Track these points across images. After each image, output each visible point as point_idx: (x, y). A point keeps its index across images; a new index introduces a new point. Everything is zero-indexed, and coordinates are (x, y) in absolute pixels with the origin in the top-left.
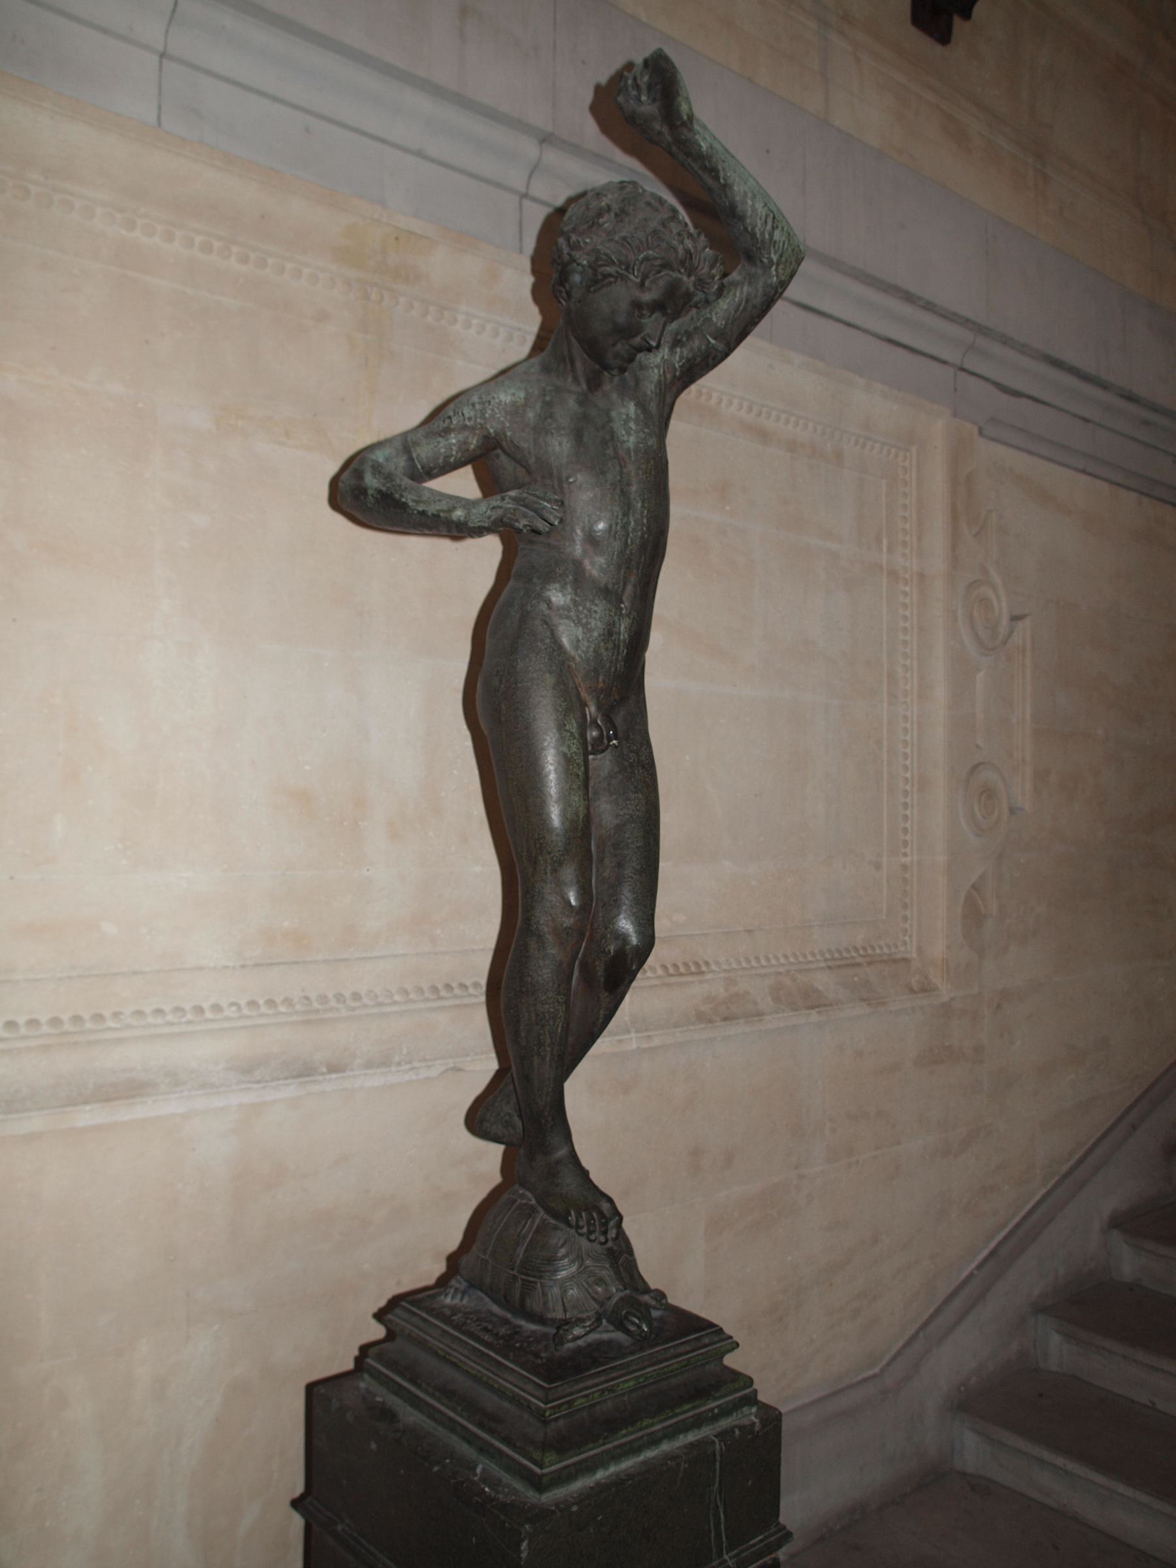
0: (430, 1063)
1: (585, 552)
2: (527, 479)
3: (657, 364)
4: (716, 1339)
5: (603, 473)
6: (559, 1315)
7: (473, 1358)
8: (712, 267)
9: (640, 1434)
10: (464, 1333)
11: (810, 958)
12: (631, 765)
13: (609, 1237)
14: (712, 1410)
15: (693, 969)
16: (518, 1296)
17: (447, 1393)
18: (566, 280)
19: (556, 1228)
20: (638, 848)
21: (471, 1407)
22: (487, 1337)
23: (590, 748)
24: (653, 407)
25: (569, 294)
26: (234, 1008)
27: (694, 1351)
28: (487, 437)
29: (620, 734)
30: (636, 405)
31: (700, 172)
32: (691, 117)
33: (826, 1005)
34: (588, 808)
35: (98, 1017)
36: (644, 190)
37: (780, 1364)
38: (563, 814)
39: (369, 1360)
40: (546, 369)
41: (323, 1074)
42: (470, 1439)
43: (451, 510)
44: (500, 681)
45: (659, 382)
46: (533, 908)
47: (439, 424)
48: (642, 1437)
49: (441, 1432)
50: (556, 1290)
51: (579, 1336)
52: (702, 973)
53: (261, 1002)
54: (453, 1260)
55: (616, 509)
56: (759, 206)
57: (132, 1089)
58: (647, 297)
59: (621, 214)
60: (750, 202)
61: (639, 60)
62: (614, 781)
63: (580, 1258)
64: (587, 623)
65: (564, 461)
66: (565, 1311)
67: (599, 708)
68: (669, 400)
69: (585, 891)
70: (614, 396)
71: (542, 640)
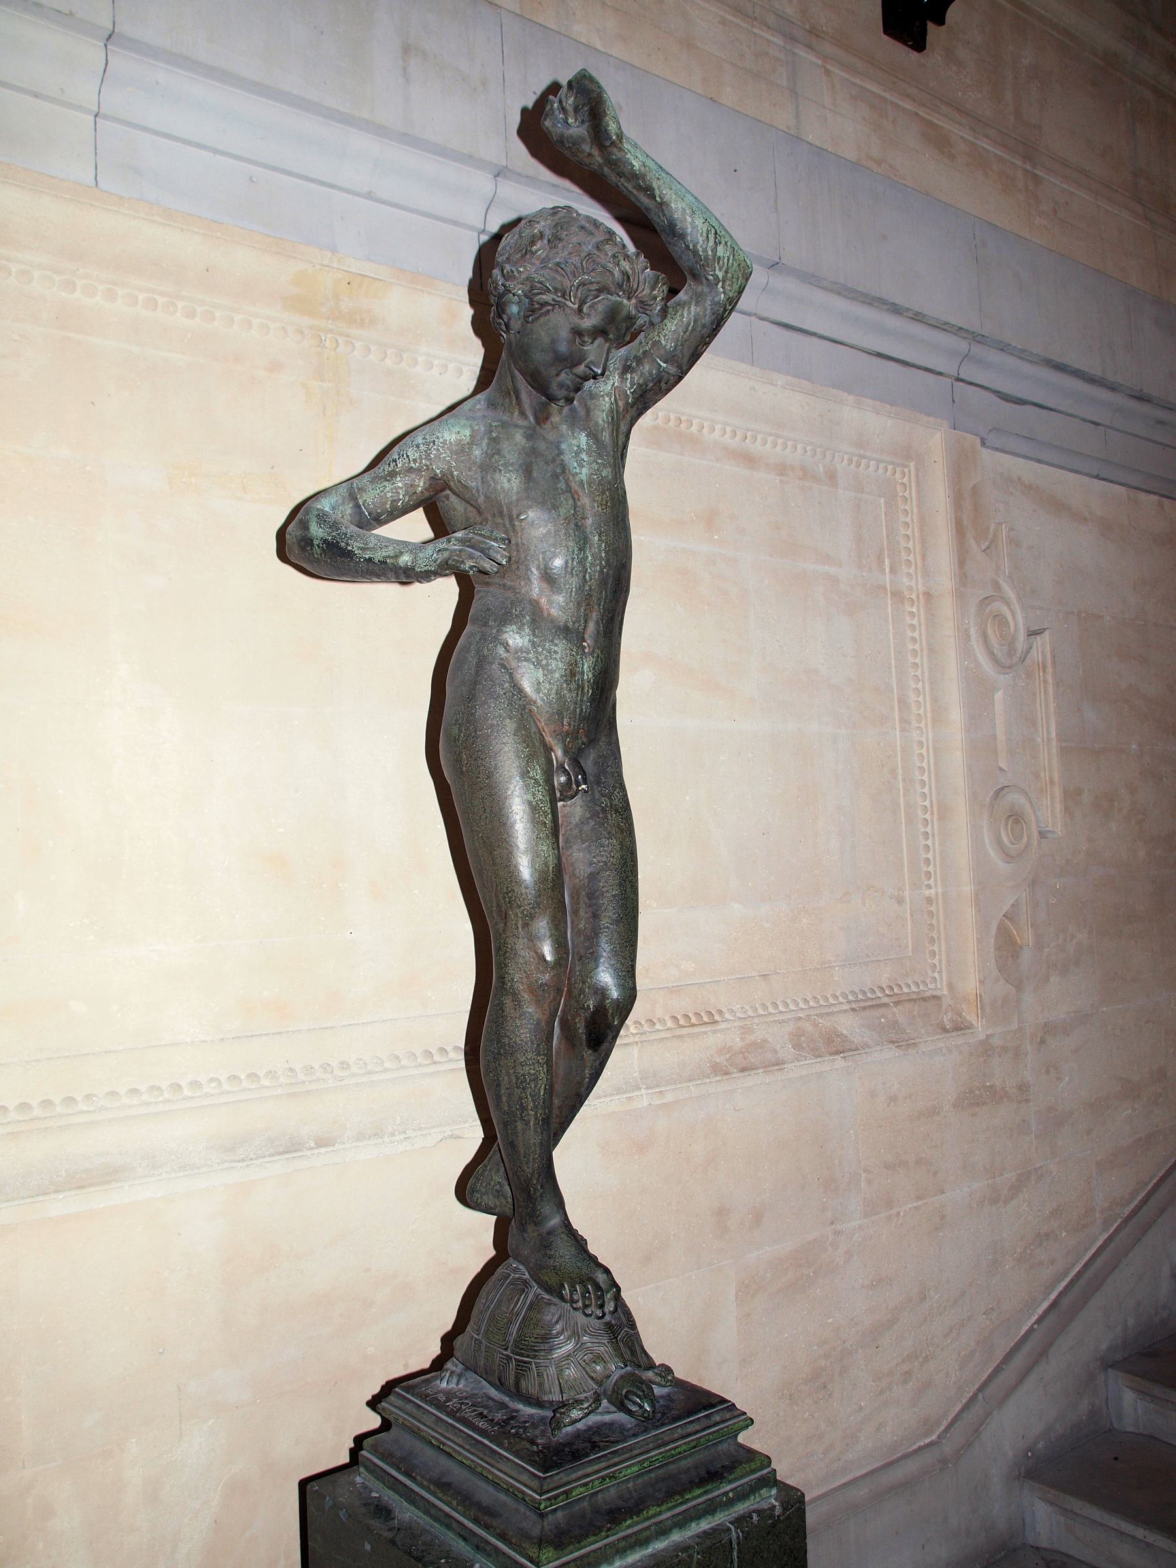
1: (541, 591)
2: (478, 519)
3: (608, 391)
4: (728, 1416)
5: (555, 507)
6: (556, 1397)
7: (467, 1447)
8: (653, 289)
9: (646, 1524)
10: (458, 1420)
11: (832, 1001)
12: (604, 810)
13: (606, 1310)
14: (726, 1493)
15: (705, 1019)
16: (512, 1377)
17: (443, 1486)
18: (504, 312)
19: (549, 1304)
20: (614, 896)
21: (466, 1501)
22: (481, 1424)
23: (558, 795)
24: (606, 437)
25: (507, 325)
26: (213, 1085)
27: (704, 1429)
28: (434, 478)
29: (590, 778)
30: (587, 436)
31: (635, 192)
32: (620, 136)
33: (850, 1050)
34: (559, 858)
35: (70, 1100)
36: (578, 214)
37: (796, 1441)
38: (532, 863)
39: (364, 1453)
40: (492, 405)
41: (312, 1149)
42: (466, 1536)
43: (396, 557)
44: (460, 731)
45: (611, 410)
46: (506, 966)
47: (384, 468)
48: (648, 1528)
49: (438, 1529)
50: (552, 1370)
51: (578, 1420)
52: (716, 1022)
53: (243, 1077)
54: (448, 1341)
55: (571, 544)
56: (699, 222)
57: (108, 1175)
58: (587, 323)
59: (555, 241)
60: (689, 219)
61: (564, 82)
62: (586, 828)
63: (575, 1334)
64: (547, 665)
65: (514, 498)
66: (562, 1392)
67: (566, 752)
68: (623, 428)
69: (560, 946)
70: (564, 427)
71: (501, 685)
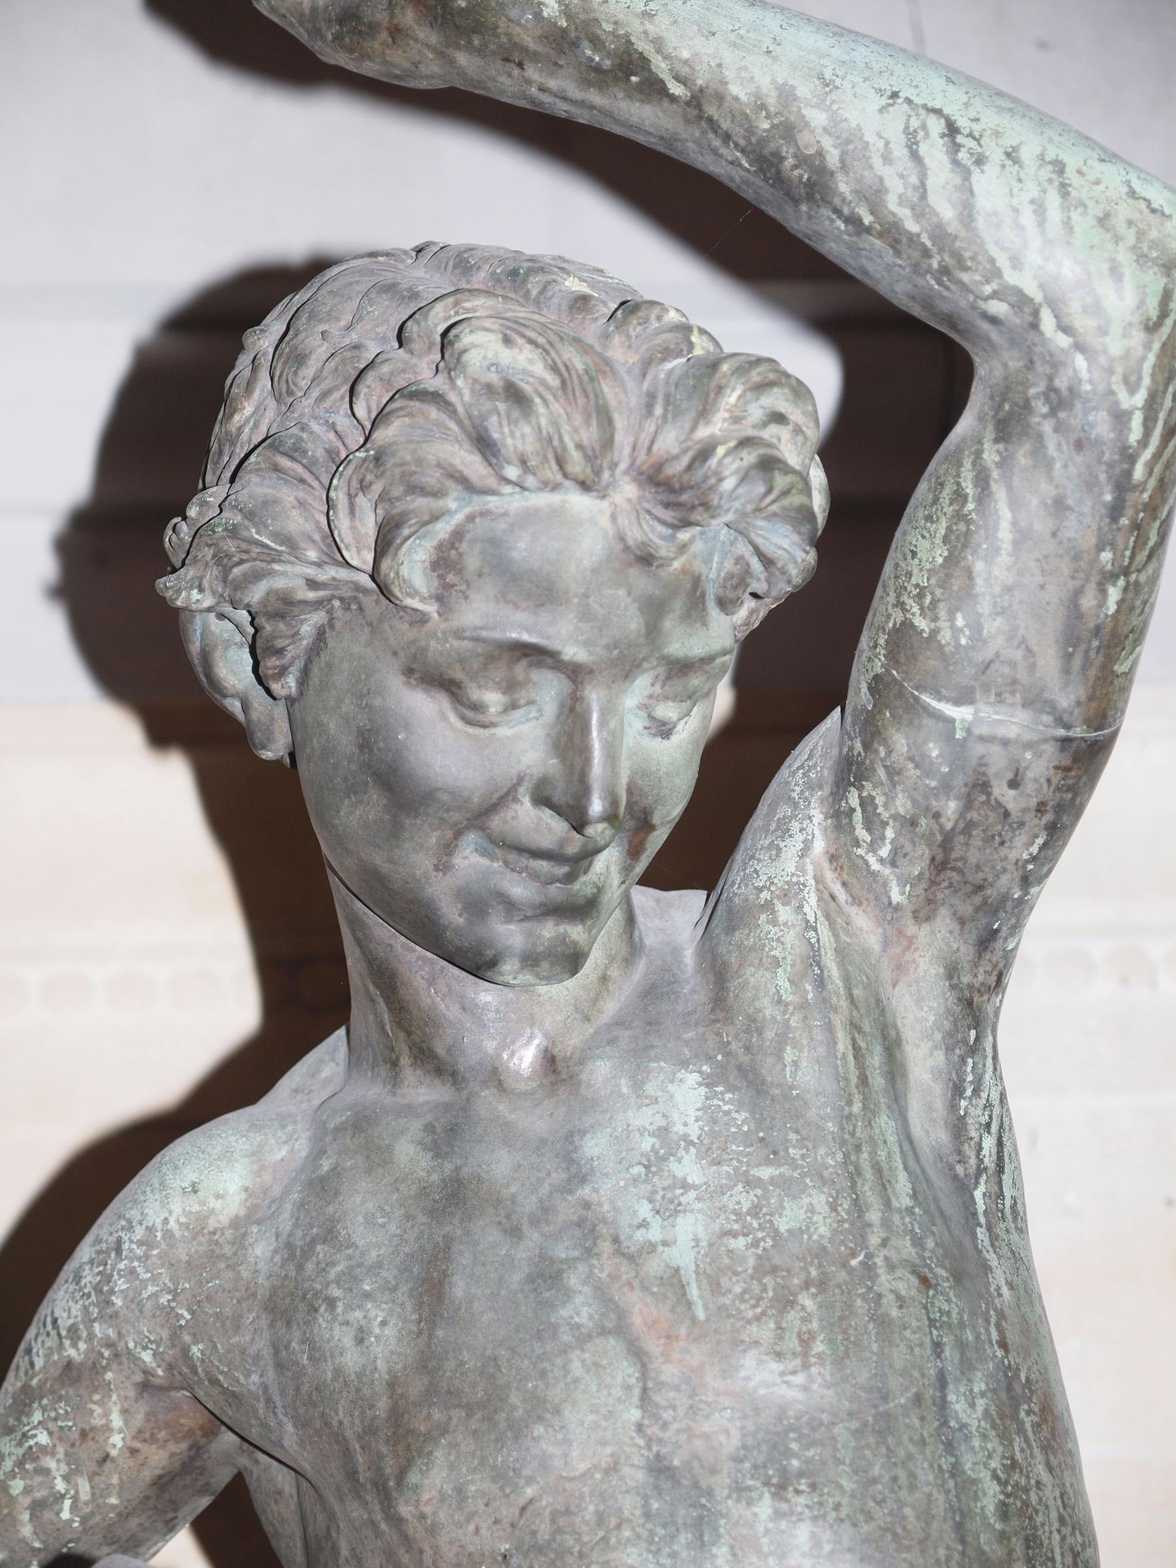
31: (595, 97)
60: (817, 118)
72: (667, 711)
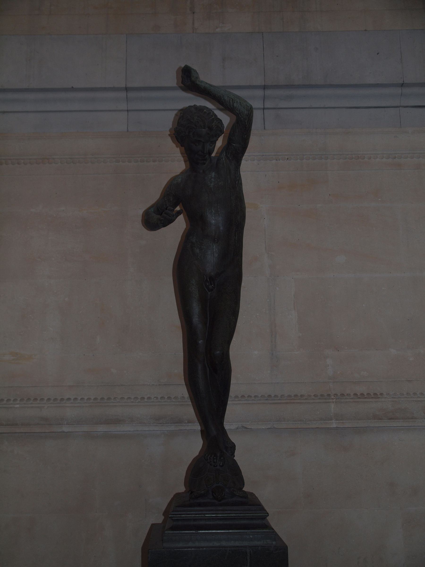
0: (231, 424)
57: (117, 421)
72: (211, 145)
